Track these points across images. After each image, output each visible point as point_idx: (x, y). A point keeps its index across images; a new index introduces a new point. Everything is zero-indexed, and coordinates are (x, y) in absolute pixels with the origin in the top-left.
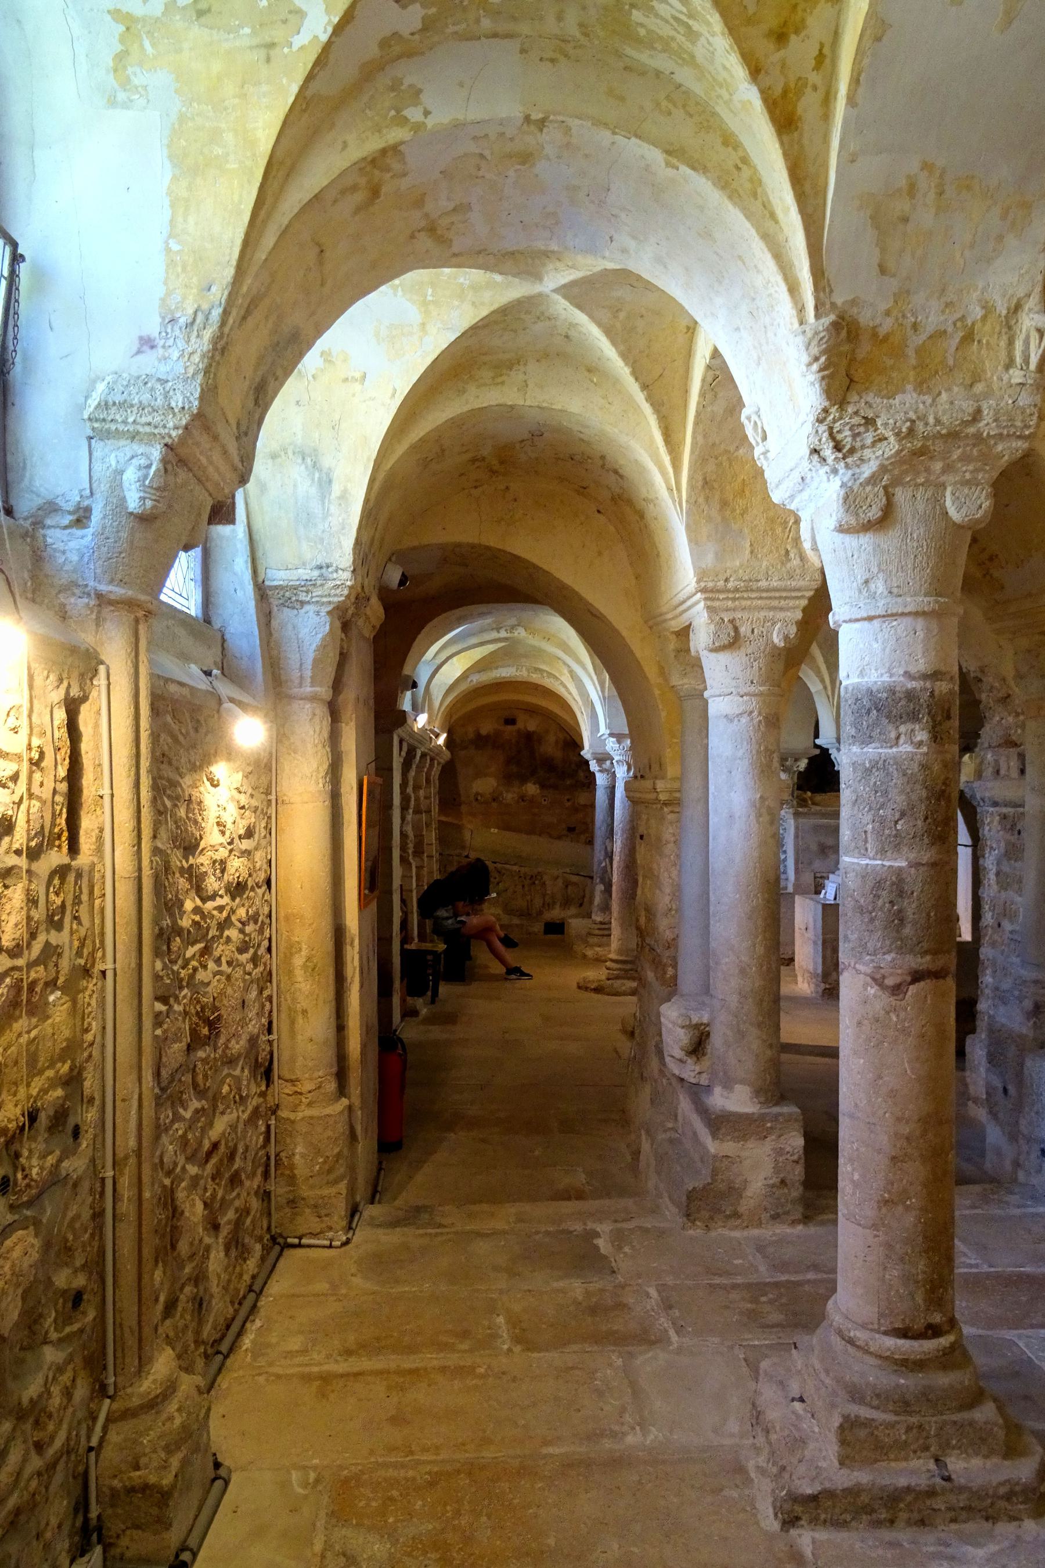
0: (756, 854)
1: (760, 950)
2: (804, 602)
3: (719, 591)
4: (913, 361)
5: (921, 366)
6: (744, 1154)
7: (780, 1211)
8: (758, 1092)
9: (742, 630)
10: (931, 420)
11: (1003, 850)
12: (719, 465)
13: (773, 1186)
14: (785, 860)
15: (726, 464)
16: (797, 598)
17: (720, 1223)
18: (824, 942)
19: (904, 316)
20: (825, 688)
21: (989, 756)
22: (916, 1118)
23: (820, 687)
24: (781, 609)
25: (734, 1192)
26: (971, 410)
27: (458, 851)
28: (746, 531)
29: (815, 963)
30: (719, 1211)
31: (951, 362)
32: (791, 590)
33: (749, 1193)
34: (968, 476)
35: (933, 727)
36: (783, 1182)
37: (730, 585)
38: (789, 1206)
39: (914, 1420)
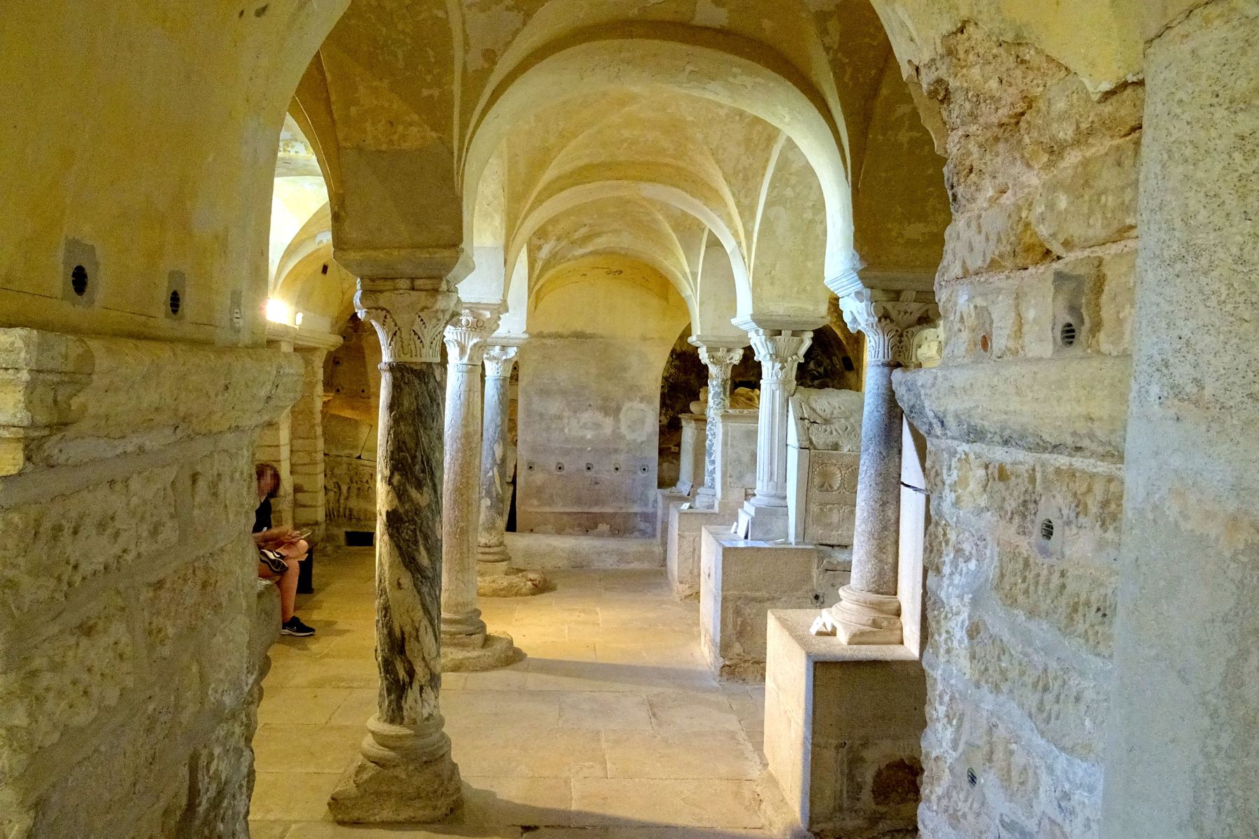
11: (992, 573)
14: (713, 471)
18: (724, 600)
20: (739, 244)
21: (962, 299)
23: (734, 243)
27: (347, 451)
29: (715, 628)
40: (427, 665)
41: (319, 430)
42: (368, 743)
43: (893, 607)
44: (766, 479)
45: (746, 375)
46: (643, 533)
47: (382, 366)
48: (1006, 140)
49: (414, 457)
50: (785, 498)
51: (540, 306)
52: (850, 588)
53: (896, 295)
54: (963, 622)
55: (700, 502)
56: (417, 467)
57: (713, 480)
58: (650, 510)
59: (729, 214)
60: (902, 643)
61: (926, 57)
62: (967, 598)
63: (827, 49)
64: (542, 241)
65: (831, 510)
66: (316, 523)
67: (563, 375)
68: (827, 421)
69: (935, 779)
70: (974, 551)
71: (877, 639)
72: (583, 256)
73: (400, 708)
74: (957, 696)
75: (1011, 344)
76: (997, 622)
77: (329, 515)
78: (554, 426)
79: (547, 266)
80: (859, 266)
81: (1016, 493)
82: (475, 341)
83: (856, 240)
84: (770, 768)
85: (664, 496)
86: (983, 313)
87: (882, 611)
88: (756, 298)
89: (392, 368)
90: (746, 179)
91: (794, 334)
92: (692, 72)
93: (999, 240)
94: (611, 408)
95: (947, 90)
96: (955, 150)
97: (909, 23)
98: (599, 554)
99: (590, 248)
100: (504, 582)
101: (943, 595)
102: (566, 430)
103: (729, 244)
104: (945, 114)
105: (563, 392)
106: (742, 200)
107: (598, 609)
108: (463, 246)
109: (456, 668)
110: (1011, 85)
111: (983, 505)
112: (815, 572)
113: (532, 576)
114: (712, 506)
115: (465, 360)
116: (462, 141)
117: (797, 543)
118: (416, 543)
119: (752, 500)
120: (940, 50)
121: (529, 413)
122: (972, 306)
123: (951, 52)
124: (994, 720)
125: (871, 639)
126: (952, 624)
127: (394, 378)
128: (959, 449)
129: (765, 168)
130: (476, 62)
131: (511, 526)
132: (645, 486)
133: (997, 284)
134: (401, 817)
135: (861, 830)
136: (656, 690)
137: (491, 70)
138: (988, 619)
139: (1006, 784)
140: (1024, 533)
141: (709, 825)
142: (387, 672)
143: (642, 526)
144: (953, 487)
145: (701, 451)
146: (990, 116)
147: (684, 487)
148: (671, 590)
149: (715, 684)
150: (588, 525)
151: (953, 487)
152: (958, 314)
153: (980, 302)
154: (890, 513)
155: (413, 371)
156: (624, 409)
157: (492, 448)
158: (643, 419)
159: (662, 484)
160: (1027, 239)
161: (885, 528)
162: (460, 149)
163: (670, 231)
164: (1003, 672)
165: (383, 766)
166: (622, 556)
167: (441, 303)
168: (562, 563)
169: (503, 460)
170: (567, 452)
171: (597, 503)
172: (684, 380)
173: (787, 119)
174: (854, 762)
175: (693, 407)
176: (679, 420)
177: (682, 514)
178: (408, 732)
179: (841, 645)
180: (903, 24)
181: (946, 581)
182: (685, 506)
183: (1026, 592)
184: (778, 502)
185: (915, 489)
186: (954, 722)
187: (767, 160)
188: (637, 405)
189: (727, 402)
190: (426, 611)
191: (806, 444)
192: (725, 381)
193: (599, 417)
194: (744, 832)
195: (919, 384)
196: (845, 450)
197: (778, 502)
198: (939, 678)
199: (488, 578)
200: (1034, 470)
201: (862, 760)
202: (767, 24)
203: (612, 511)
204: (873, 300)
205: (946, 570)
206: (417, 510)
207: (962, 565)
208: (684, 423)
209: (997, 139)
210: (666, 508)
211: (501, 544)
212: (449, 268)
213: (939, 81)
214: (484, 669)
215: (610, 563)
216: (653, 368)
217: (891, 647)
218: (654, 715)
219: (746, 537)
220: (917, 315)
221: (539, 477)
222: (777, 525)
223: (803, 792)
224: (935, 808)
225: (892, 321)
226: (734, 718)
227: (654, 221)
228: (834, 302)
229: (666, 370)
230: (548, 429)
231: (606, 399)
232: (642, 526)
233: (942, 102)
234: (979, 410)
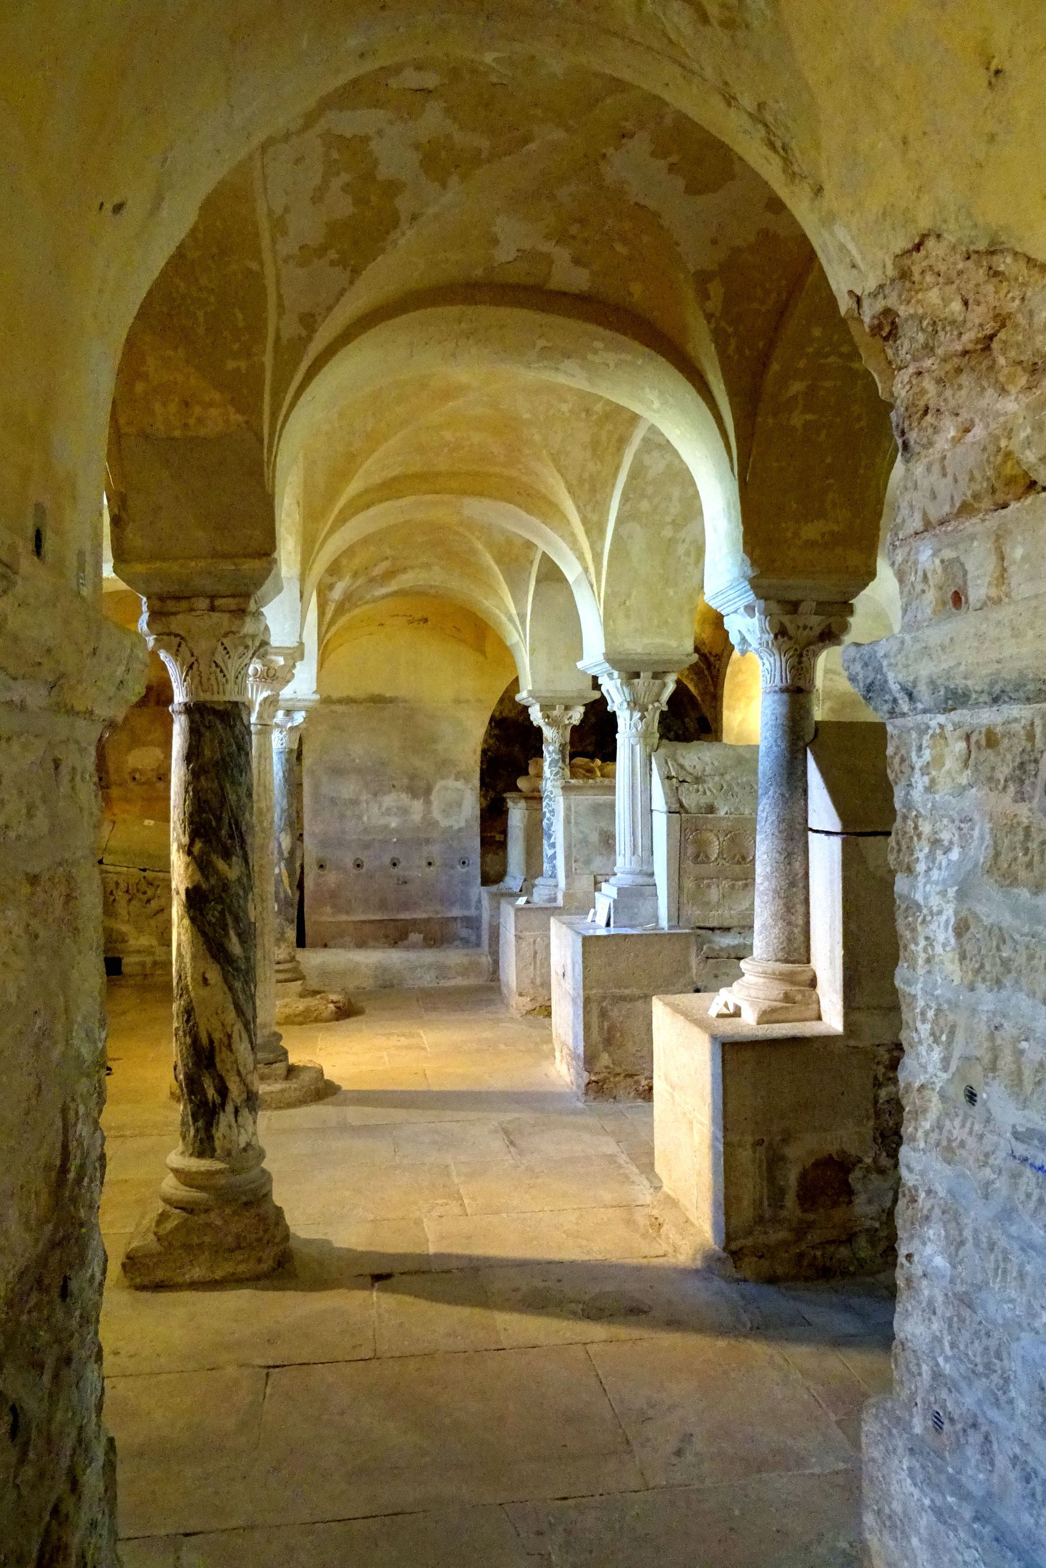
11: (981, 853)
14: (554, 857)
18: (587, 1001)
20: (586, 570)
29: (575, 1037)
42: (170, 1184)
43: (806, 977)
44: (628, 855)
45: (594, 738)
46: (466, 942)
48: (973, 369)
49: (219, 819)
50: (652, 874)
51: (326, 665)
52: (754, 959)
53: (793, 607)
54: (947, 922)
55: (540, 896)
56: (223, 832)
57: (554, 867)
58: (472, 912)
59: (573, 535)
60: (819, 1018)
61: (872, 285)
62: (952, 892)
63: (709, 317)
64: (335, 579)
65: (709, 886)
67: (359, 748)
68: (698, 780)
69: (920, 1112)
70: (956, 839)
71: (791, 1016)
72: (384, 597)
73: (211, 1138)
74: (946, 1006)
75: (993, 592)
76: (992, 908)
78: (349, 813)
79: (341, 608)
80: (750, 573)
81: (1009, 757)
82: (266, 694)
83: (745, 543)
84: (665, 1189)
85: (489, 893)
86: (953, 568)
87: (793, 983)
88: (609, 634)
89: (188, 710)
90: (593, 490)
91: (656, 676)
92: (544, 348)
93: (972, 479)
94: (419, 788)
95: (893, 323)
96: (903, 393)
97: (851, 246)
98: (413, 969)
99: (393, 586)
100: (301, 1005)
101: (919, 897)
102: (365, 818)
103: (571, 571)
104: (890, 352)
105: (359, 771)
106: (589, 515)
107: (422, 1033)
108: (275, 555)
110: (979, 304)
111: (965, 782)
112: (694, 961)
113: (333, 997)
114: (555, 900)
117: (670, 927)
118: (225, 927)
119: (612, 880)
120: (891, 272)
121: (316, 796)
122: (937, 561)
123: (904, 275)
124: (998, 1020)
125: (781, 1017)
126: (933, 926)
127: (192, 721)
128: (933, 723)
129: (615, 476)
130: (291, 328)
131: (301, 943)
132: (466, 883)
133: (970, 530)
134: (218, 1275)
135: (785, 1244)
136: (509, 1116)
137: (309, 338)
138: (980, 909)
139: (1017, 1089)
140: (1023, 800)
141: (600, 1257)
142: (191, 1092)
143: (464, 932)
144: (925, 770)
145: (536, 833)
146: (949, 343)
147: (514, 880)
148: (507, 1006)
149: (580, 1105)
150: (396, 934)
151: (925, 770)
152: (920, 573)
153: (948, 554)
154: (797, 865)
155: (215, 712)
156: (434, 792)
158: (460, 802)
159: (486, 881)
160: (1008, 470)
161: (792, 884)
162: (271, 435)
163: (492, 563)
164: (1006, 963)
165: (191, 1212)
166: (442, 971)
168: (368, 984)
169: (292, 852)
170: (367, 846)
171: (405, 906)
172: (510, 747)
173: (656, 405)
174: (774, 1162)
175: (522, 783)
176: (503, 801)
177: (519, 910)
178: (219, 1165)
179: (749, 1024)
180: (842, 247)
181: (921, 880)
182: (521, 901)
183: (1030, 865)
184: (646, 880)
185: (828, 833)
186: (944, 1038)
187: (617, 468)
188: (451, 783)
189: (567, 772)
190: (240, 1011)
191: (675, 807)
192: (563, 746)
193: (405, 798)
194: (645, 1261)
195: (881, 654)
196: (722, 813)
197: (646, 880)
198: (919, 993)
200: (1032, 724)
201: (783, 1158)
202: (637, 289)
203: (424, 916)
204: (767, 613)
205: (921, 867)
206: (225, 887)
207: (940, 856)
208: (510, 804)
209: (959, 371)
210: (496, 910)
212: (259, 584)
213: (887, 312)
214: (290, 1105)
215: (428, 980)
216: (469, 738)
217: (808, 1023)
218: (512, 1143)
219: (608, 925)
220: (817, 631)
221: (332, 878)
222: (645, 909)
223: (715, 1204)
224: (922, 1145)
225: (790, 638)
226: (612, 1141)
227: (474, 551)
228: (718, 619)
229: (485, 741)
230: (342, 817)
231: (412, 778)
232: (464, 932)
233: (886, 339)
234: (962, 668)
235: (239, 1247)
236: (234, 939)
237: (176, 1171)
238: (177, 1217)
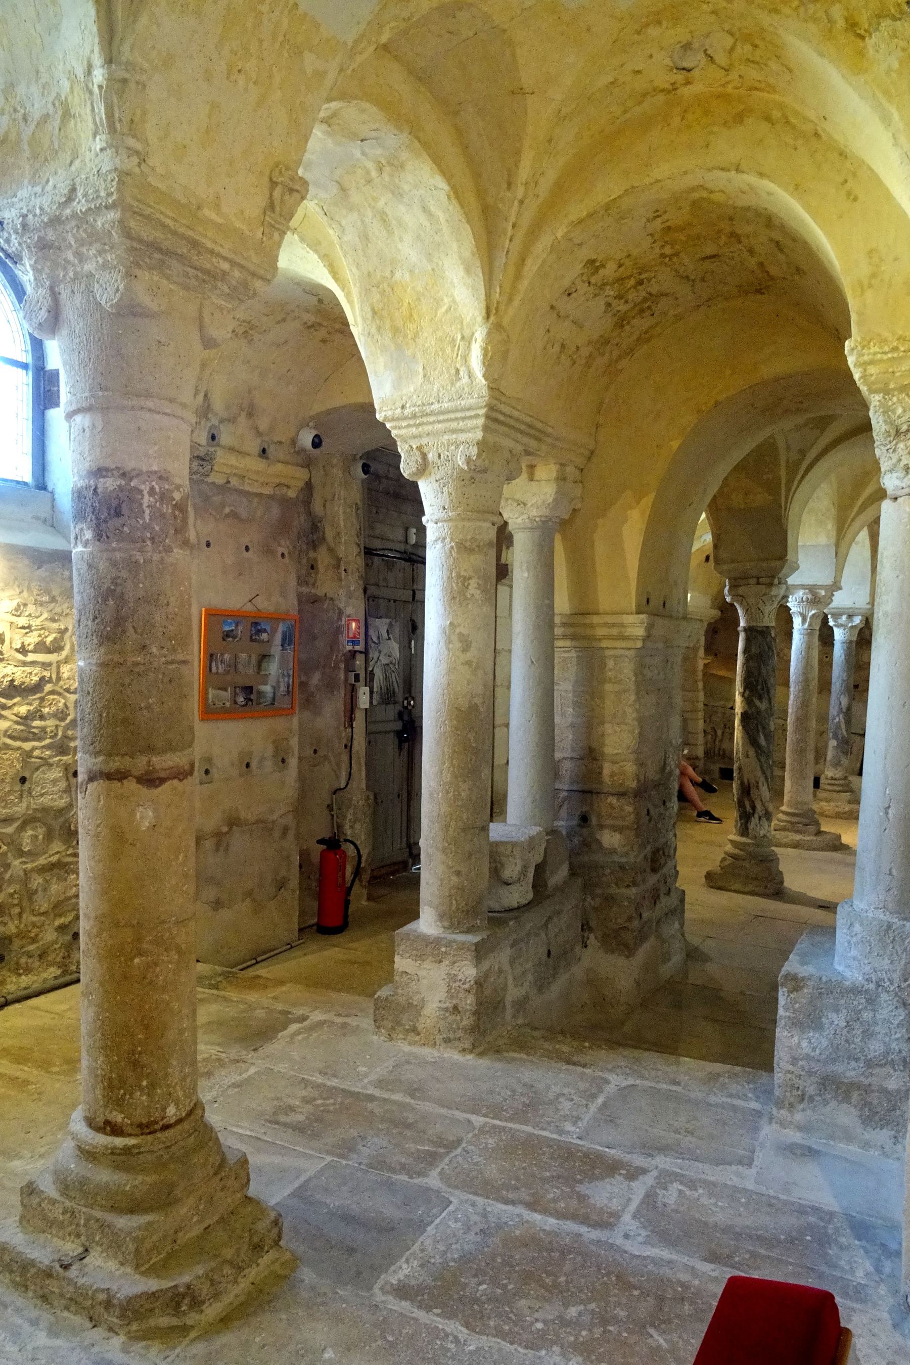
0: (444, 681)
1: (447, 777)
2: (481, 421)
3: (398, 419)
4: (27, 154)
5: (35, 156)
6: (422, 973)
7: (452, 1036)
8: (441, 917)
9: (430, 456)
10: (38, 211)
12: (383, 293)
13: (446, 1010)
15: (388, 290)
16: (470, 417)
17: (401, 1036)
19: (15, 110)
22: (93, 915)
24: (462, 431)
25: (413, 1008)
26: (66, 192)
27: (722, 703)
28: (419, 355)
30: (399, 1023)
31: (56, 147)
32: (462, 410)
33: (427, 1011)
34: (100, 260)
35: (98, 525)
36: (455, 1008)
37: (407, 412)
38: (460, 1034)
39: (68, 1204)
40: (763, 804)
41: (701, 685)
42: (729, 848)
47: (739, 629)
49: (757, 681)
66: (697, 758)
73: (747, 828)
77: (707, 753)
89: (745, 629)
109: (796, 845)
115: (806, 625)
116: (787, 498)
118: (758, 731)
137: (803, 459)
155: (757, 631)
157: (838, 699)
167: (774, 591)
169: (849, 709)
178: (749, 841)
199: (832, 804)
206: (759, 712)
211: (846, 778)
214: (814, 850)
235: (756, 879)
236: (762, 737)
237: (731, 841)
238: (730, 860)
